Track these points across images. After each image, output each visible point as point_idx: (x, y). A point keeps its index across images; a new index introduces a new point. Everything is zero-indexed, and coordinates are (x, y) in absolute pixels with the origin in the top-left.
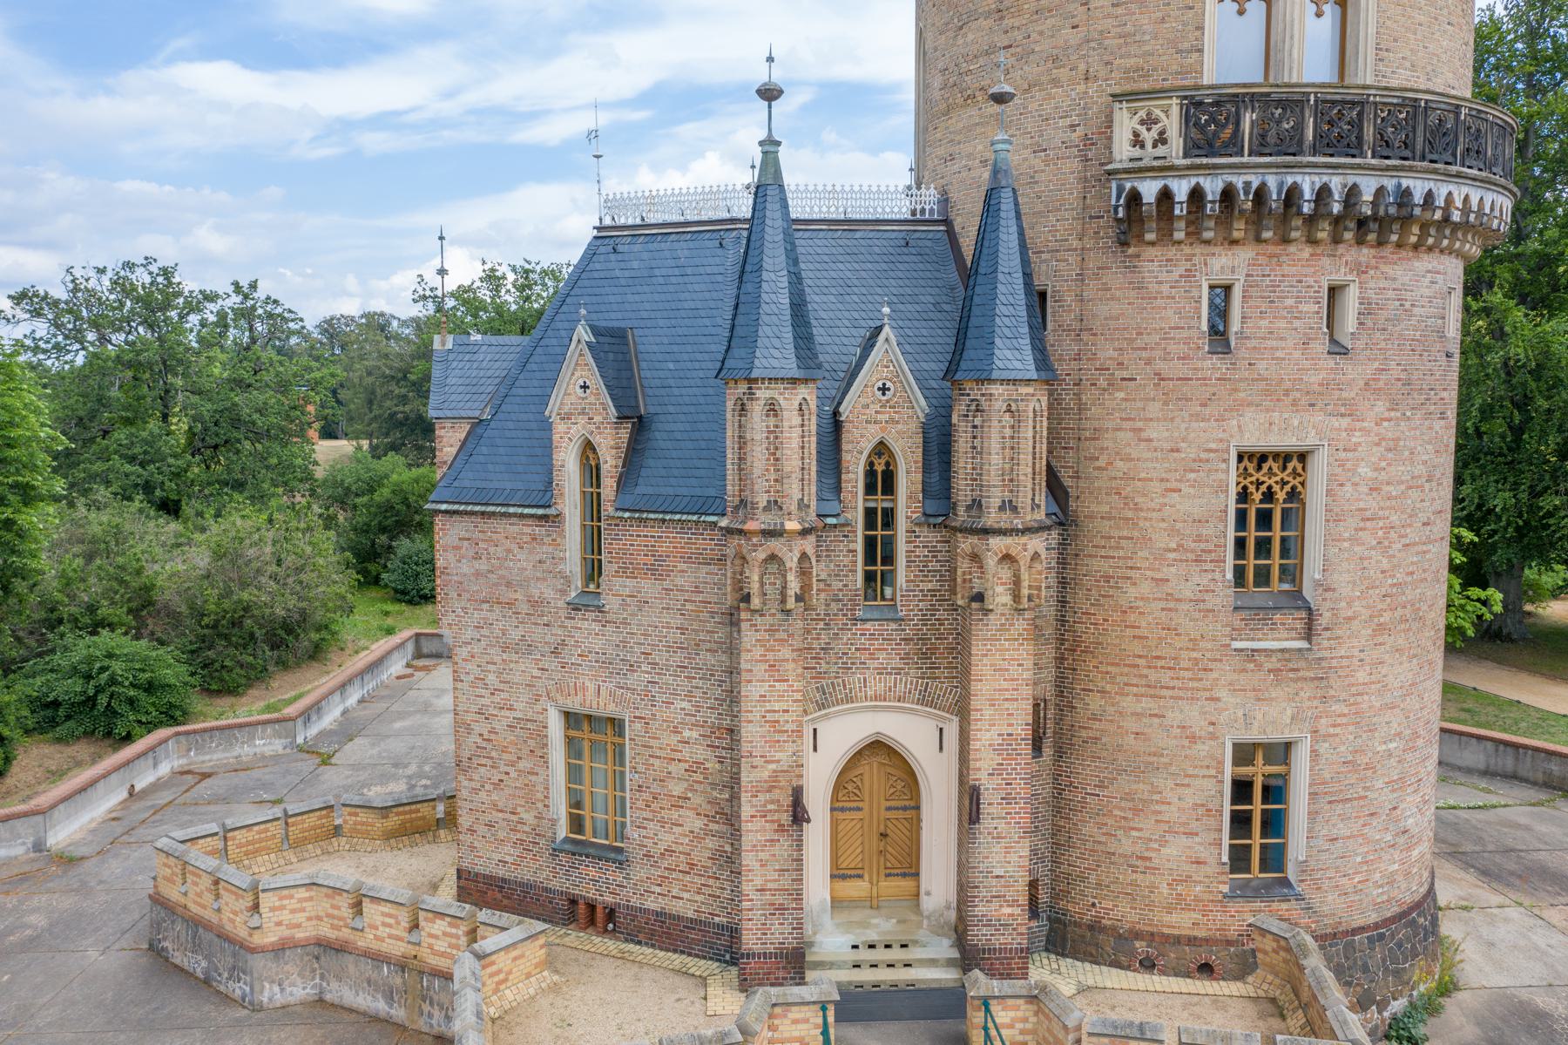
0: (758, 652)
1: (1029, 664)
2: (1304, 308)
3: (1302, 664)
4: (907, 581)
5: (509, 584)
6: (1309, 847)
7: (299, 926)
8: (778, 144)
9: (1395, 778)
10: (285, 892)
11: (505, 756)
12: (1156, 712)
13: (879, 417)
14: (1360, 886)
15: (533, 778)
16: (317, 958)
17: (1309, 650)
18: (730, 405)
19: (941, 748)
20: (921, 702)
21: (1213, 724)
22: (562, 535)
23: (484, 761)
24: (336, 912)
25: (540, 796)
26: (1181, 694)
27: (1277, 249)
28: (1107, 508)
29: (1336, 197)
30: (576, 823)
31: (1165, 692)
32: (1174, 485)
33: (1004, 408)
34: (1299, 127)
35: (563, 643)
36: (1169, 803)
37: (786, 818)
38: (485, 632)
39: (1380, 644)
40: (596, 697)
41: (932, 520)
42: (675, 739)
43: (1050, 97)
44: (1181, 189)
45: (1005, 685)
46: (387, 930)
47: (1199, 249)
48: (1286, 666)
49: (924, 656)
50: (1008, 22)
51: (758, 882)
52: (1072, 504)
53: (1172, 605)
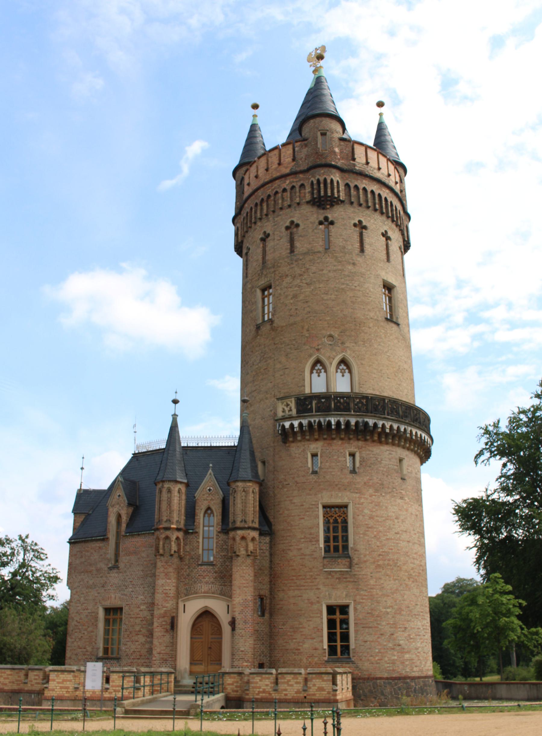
0: (162, 569)
1: (252, 574)
2: (340, 459)
3: (348, 576)
4: (216, 552)
5: (91, 565)
6: (356, 643)
7: (6, 684)
8: (177, 416)
9: (392, 623)
10: (3, 671)
11: (84, 627)
12: (299, 595)
13: (208, 498)
14: (378, 661)
15: (92, 634)
16: (10, 697)
17: (351, 571)
18: (157, 491)
19: (228, 613)
20: (220, 594)
21: (318, 598)
22: (108, 545)
23: (76, 630)
24: (19, 679)
25: (94, 640)
26: (307, 587)
27: (331, 442)
29: (342, 423)
30: (106, 650)
32: (302, 517)
33: (242, 490)
34: (330, 405)
35: (106, 582)
36: (305, 628)
37: (169, 627)
38: (81, 583)
39: (379, 572)
40: (114, 601)
41: (224, 531)
42: (138, 610)
44: (296, 423)
45: (244, 582)
46: (35, 681)
47: (306, 443)
48: (342, 577)
49: (222, 578)
50: (256, 383)
51: (158, 650)
52: (273, 527)
53: (303, 557)
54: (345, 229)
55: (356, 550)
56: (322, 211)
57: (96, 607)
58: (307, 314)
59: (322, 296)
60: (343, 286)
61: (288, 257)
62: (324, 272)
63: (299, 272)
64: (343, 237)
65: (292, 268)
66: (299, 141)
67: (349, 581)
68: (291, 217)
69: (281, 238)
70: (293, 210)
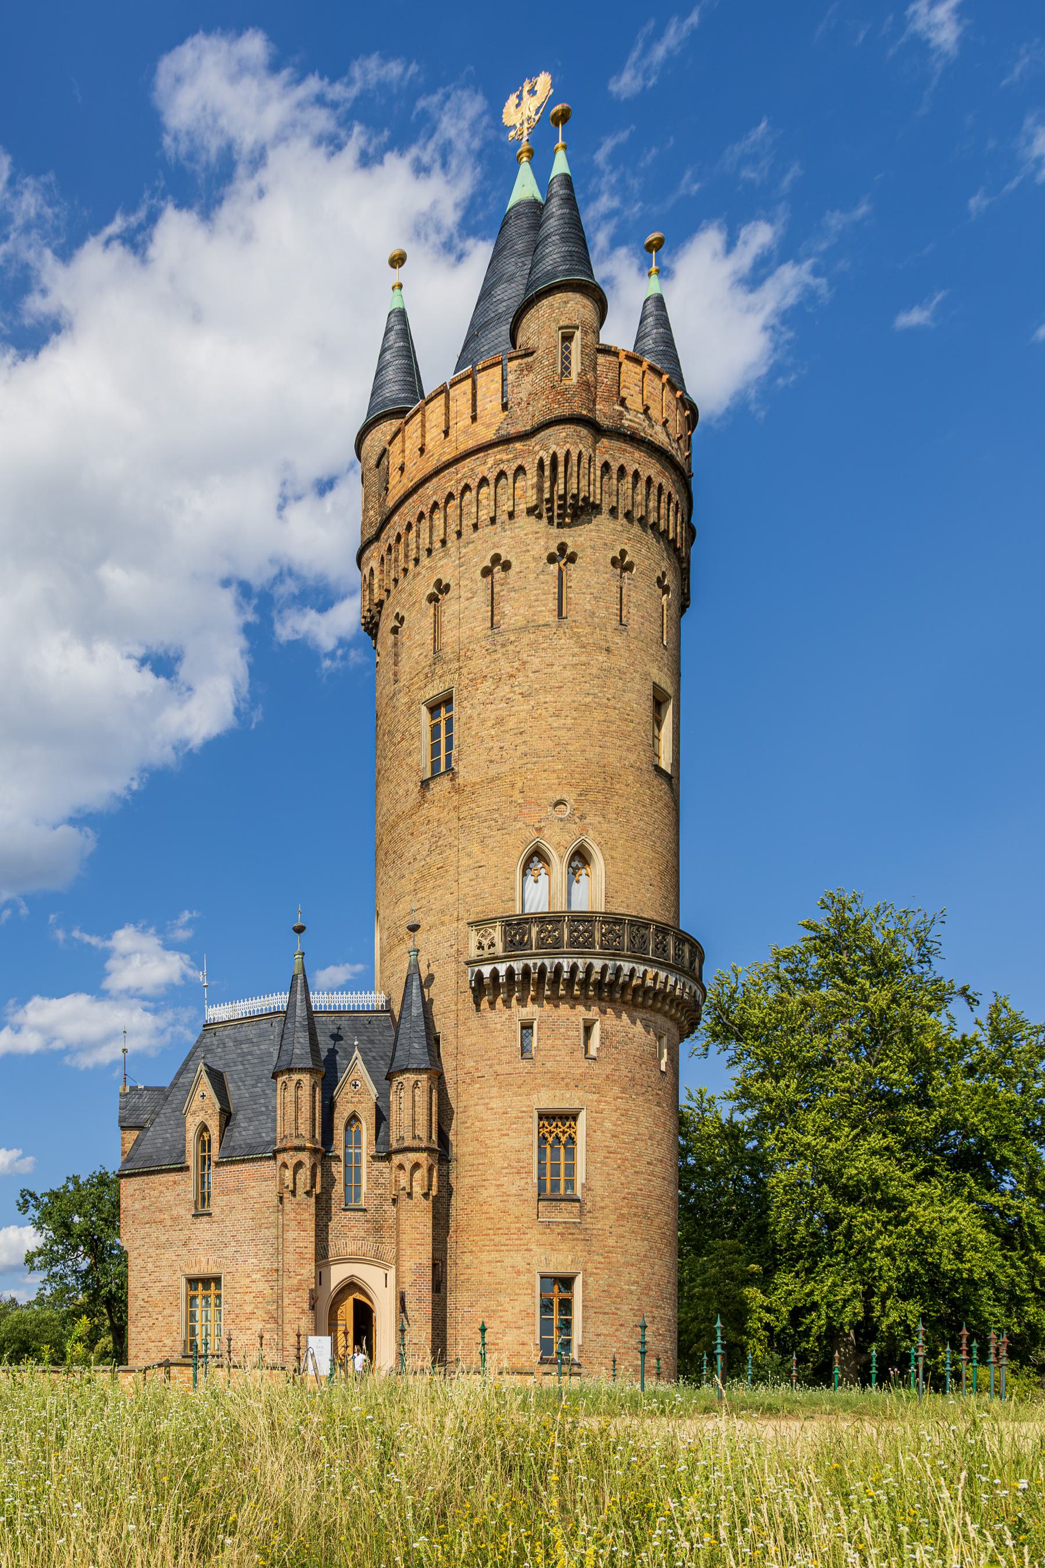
28: (471, 1149)
31: (503, 1248)
40: (204, 1267)
43: (440, 932)
54: (597, 571)
55: (589, 1190)
56: (554, 531)
57: (175, 1278)
58: (521, 758)
59: (550, 719)
60: (588, 699)
61: (486, 637)
62: (555, 668)
63: (510, 670)
64: (592, 591)
65: (495, 660)
66: (517, 358)
67: (578, 1240)
68: (495, 546)
69: (474, 594)
70: (499, 529)
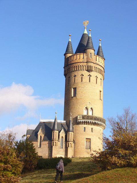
44: (82, 121)
